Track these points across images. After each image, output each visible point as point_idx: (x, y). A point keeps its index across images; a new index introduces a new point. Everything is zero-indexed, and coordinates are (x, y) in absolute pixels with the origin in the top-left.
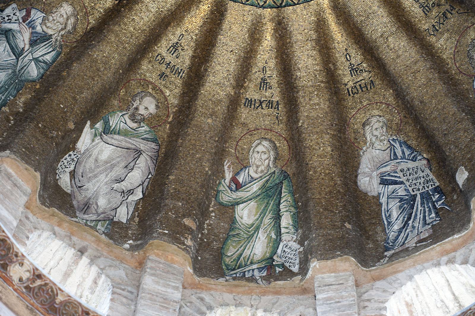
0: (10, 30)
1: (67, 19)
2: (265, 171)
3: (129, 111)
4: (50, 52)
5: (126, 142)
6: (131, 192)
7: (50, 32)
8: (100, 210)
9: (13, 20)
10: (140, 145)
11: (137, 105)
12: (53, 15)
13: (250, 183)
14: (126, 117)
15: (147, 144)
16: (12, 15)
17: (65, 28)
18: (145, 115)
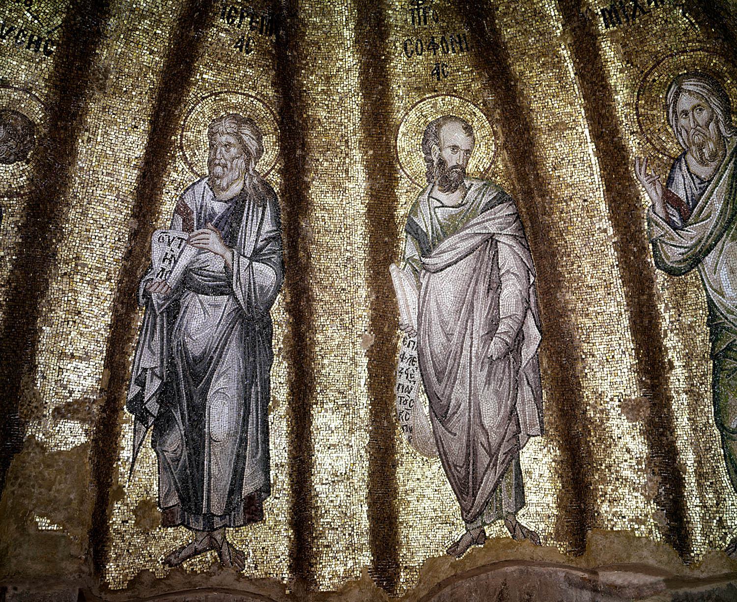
0: (187, 271)
1: (240, 140)
2: (720, 153)
3: (433, 177)
4: (263, 214)
5: (463, 240)
6: (520, 337)
7: (236, 189)
8: (494, 438)
9: (177, 252)
10: (486, 228)
11: (437, 155)
12: (217, 162)
13: (702, 194)
14: (437, 193)
15: (495, 215)
16: (167, 249)
17: (248, 153)
18: (461, 163)
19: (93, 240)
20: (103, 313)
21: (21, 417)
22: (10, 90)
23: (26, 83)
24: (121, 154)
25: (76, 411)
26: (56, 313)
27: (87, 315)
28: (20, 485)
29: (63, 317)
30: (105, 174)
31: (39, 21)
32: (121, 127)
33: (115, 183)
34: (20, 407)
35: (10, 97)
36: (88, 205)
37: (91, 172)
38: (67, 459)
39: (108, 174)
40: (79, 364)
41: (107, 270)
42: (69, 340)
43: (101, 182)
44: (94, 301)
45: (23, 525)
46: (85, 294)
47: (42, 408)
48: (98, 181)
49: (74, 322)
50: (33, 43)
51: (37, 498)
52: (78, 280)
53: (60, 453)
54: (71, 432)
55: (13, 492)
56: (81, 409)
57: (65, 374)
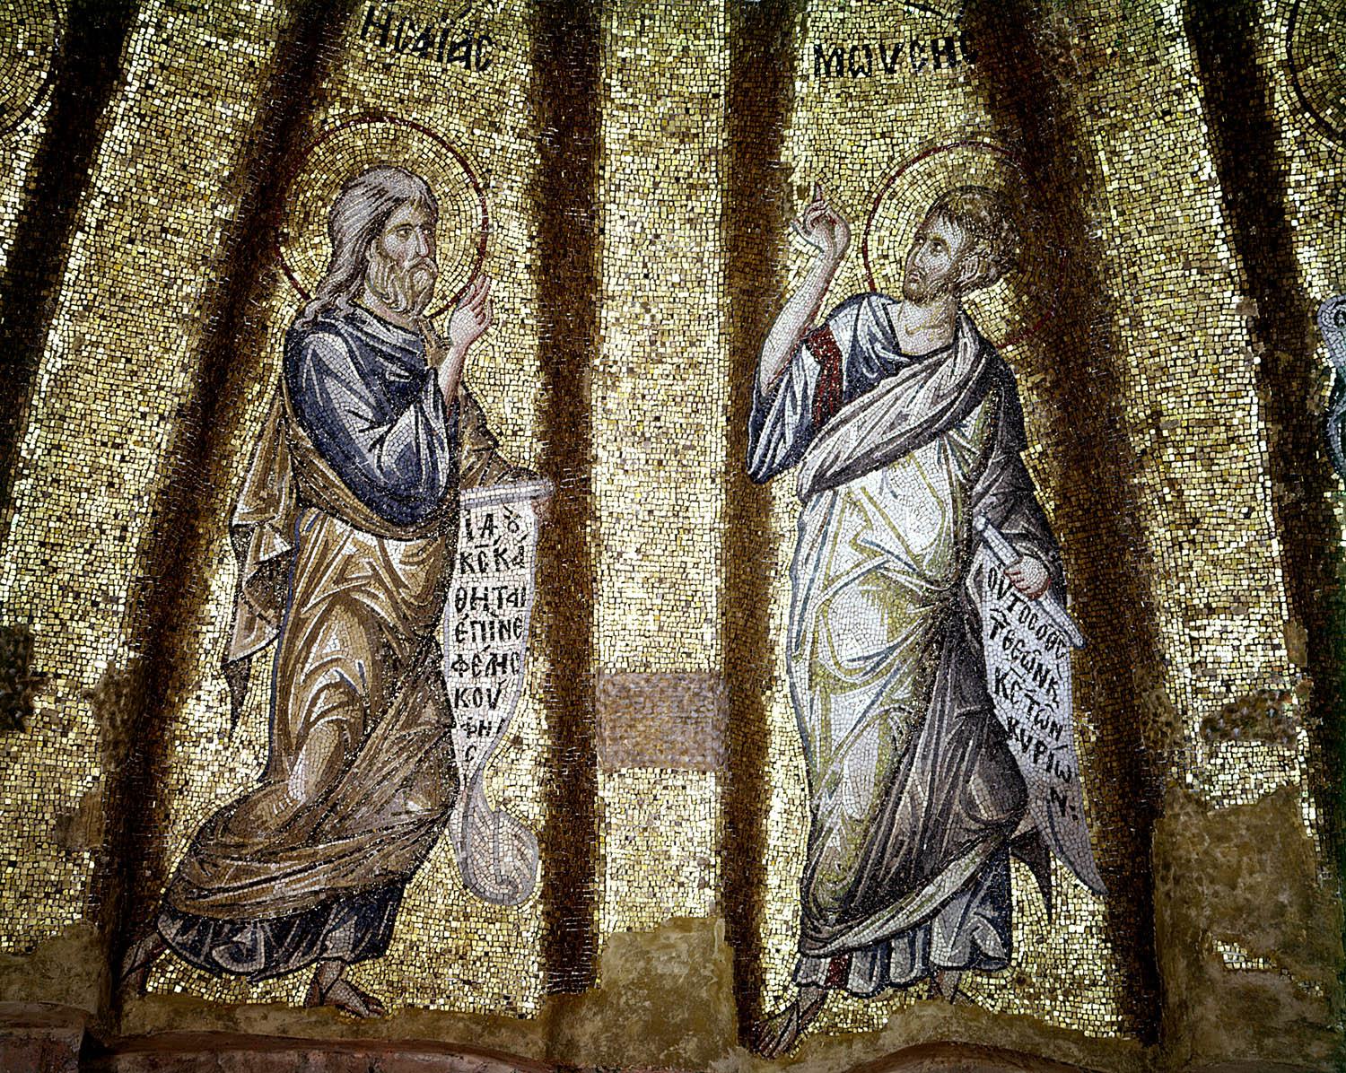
19: (1171, 370)
20: (1245, 510)
21: (1148, 747)
22: (941, 154)
23: (961, 129)
24: (1161, 181)
25: (1248, 722)
26: (1152, 533)
27: (1214, 521)
28: (1177, 881)
29: (1169, 537)
30: (1144, 233)
31: (933, 11)
32: (1137, 127)
33: (1171, 243)
34: (1142, 728)
35: (947, 167)
36: (1136, 306)
37: (1118, 241)
38: (1255, 821)
39: (1151, 230)
40: (1228, 623)
41: (1222, 422)
42: (1194, 580)
43: (1143, 252)
44: (1218, 491)
45: (1197, 959)
46: (1194, 481)
47: (1180, 724)
48: (1138, 252)
49: (1193, 542)
50: (942, 53)
51: (1210, 904)
52: (1172, 458)
53: (1237, 810)
54: (1250, 766)
55: (1168, 894)
56: (1257, 714)
57: (1205, 648)
